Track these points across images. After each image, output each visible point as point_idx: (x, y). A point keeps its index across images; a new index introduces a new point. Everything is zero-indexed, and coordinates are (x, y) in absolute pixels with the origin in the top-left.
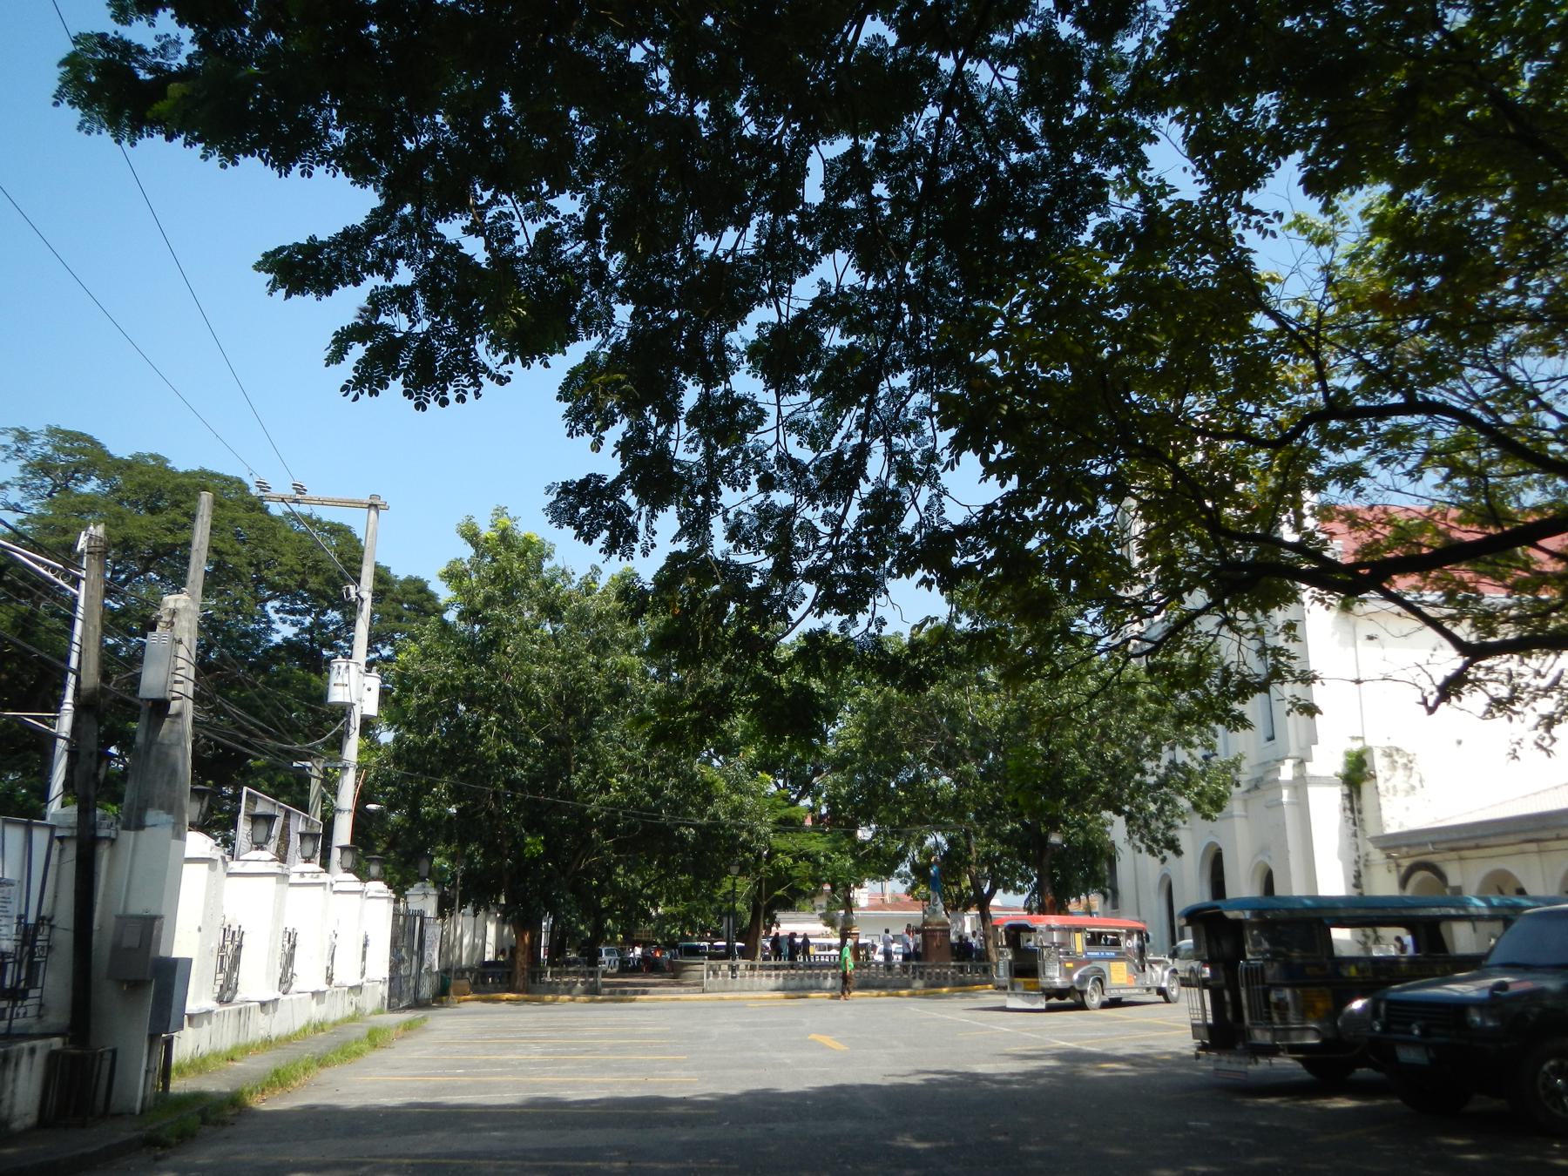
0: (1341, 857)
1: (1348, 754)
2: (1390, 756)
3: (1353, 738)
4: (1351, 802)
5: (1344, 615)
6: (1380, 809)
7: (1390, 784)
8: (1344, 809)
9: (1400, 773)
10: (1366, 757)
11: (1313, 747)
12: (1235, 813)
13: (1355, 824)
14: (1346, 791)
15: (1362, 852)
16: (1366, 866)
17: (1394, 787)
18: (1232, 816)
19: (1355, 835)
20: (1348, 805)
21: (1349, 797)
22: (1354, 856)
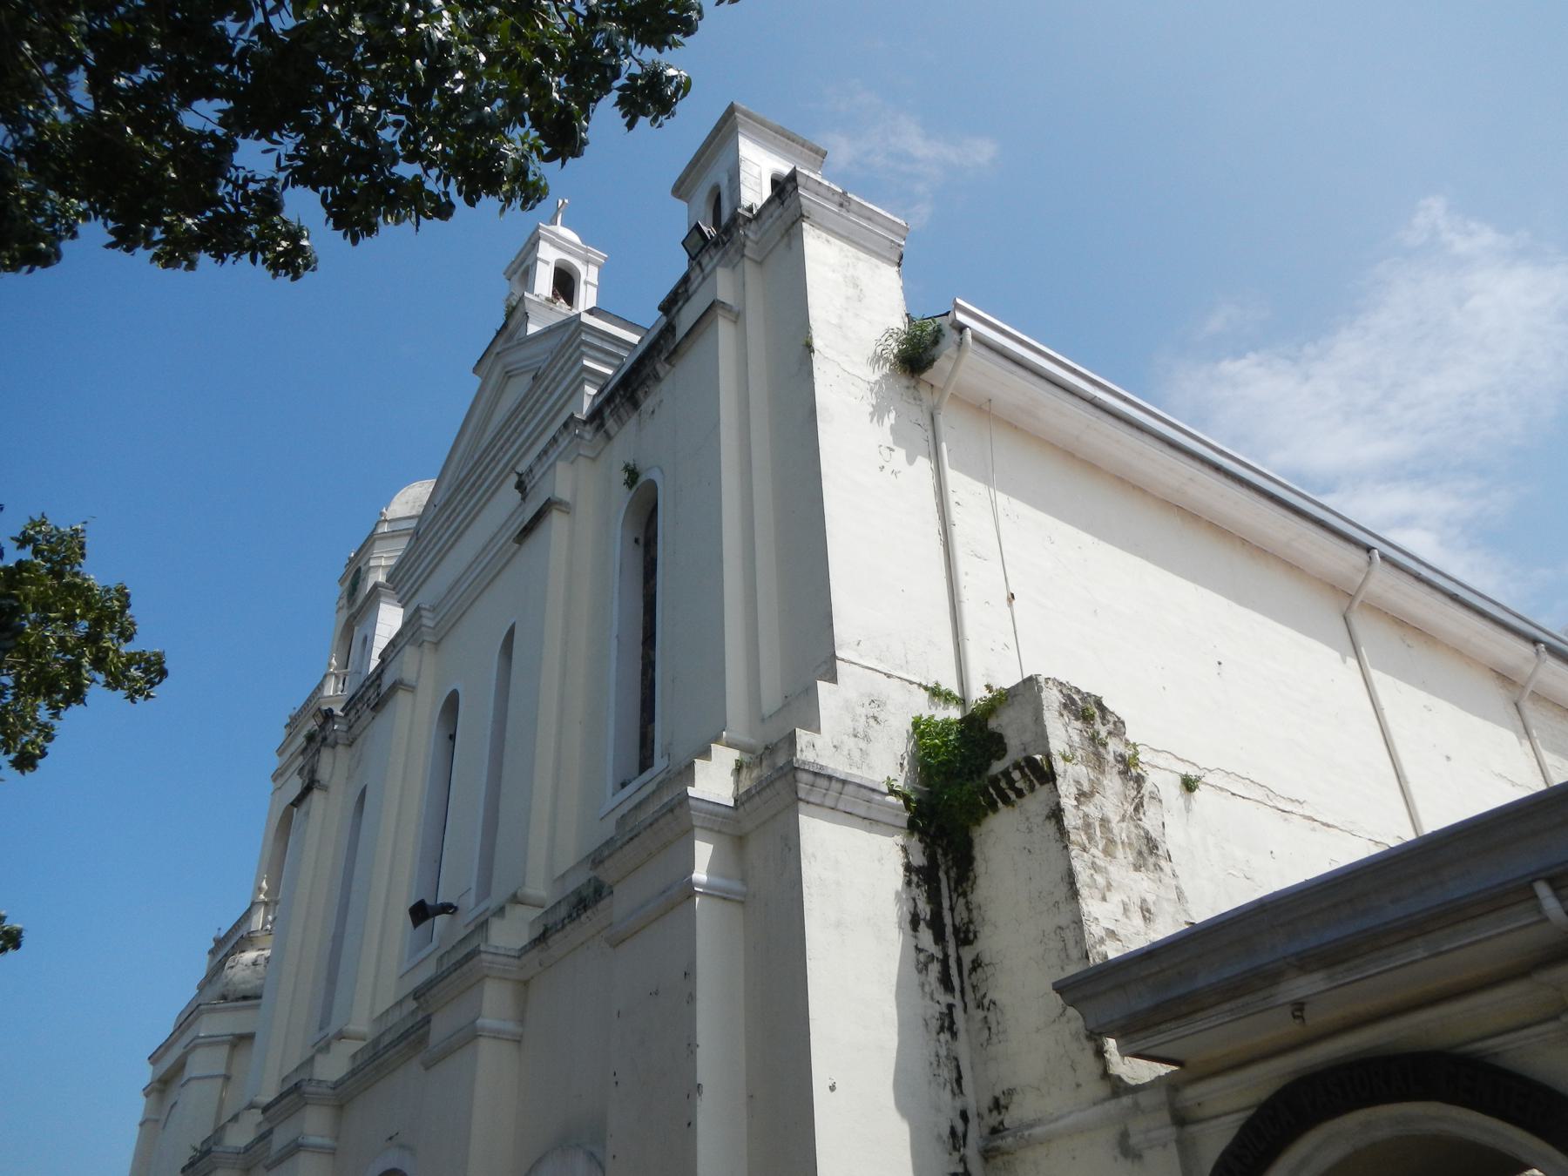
0: (903, 1107)
1: (920, 729)
2: (1086, 717)
3: (935, 693)
4: (934, 897)
5: (904, 381)
6: (1074, 894)
7: (1089, 809)
8: (915, 921)
9: (1112, 783)
10: (1005, 723)
11: (823, 687)
12: (487, 1021)
13: (946, 981)
14: (919, 860)
15: (974, 1099)
16: (987, 1154)
17: (1104, 822)
18: (470, 1035)
19: (947, 1024)
20: (925, 910)
21: (922, 876)
22: (948, 1106)
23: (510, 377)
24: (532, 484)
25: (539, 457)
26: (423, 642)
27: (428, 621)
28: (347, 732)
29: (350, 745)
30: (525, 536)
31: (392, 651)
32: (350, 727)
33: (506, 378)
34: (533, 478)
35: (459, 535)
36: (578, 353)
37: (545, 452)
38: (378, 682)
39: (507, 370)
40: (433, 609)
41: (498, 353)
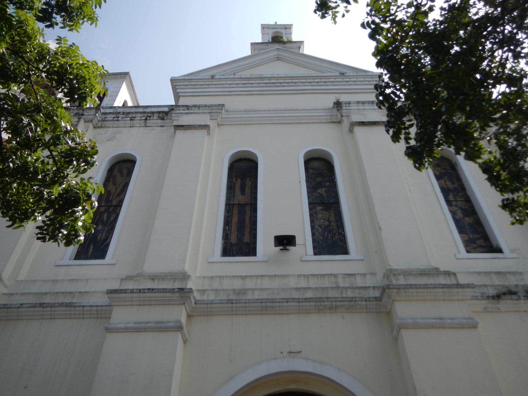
23: (278, 60)
24: (348, 108)
25: (358, 102)
26: (216, 119)
27: (224, 114)
28: (99, 121)
29: (95, 128)
30: (359, 125)
31: (184, 110)
32: (103, 121)
34: (349, 106)
35: (250, 94)
37: (364, 103)
38: (149, 115)
39: (279, 56)
40: (227, 111)
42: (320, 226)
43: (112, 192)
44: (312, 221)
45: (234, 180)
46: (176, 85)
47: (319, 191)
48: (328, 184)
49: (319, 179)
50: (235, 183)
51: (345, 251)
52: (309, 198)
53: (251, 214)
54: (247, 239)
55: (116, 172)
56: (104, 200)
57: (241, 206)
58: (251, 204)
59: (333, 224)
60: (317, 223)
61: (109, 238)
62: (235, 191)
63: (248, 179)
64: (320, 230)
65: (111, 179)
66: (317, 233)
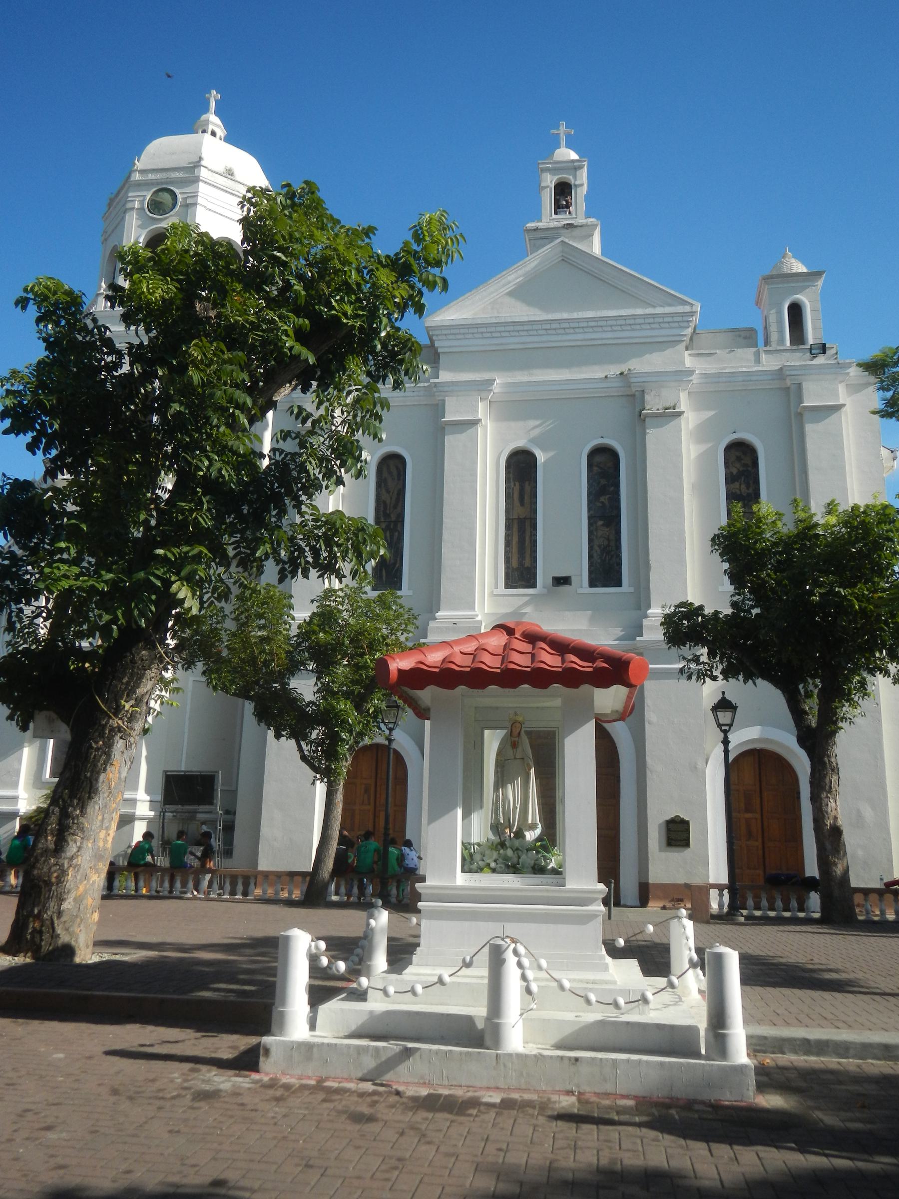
33: (560, 259)
36: (685, 324)
41: (562, 241)
42: (599, 546)
43: (388, 502)
44: (590, 541)
45: (512, 484)
46: (433, 335)
47: (602, 499)
48: (612, 489)
49: (603, 482)
50: (513, 489)
51: (619, 584)
52: (589, 511)
53: (531, 532)
54: (527, 563)
55: (385, 474)
56: (382, 513)
57: (522, 522)
58: (530, 518)
59: (613, 544)
60: (596, 542)
61: (398, 562)
62: (513, 500)
63: (527, 483)
64: (599, 551)
65: (383, 485)
66: (595, 555)
